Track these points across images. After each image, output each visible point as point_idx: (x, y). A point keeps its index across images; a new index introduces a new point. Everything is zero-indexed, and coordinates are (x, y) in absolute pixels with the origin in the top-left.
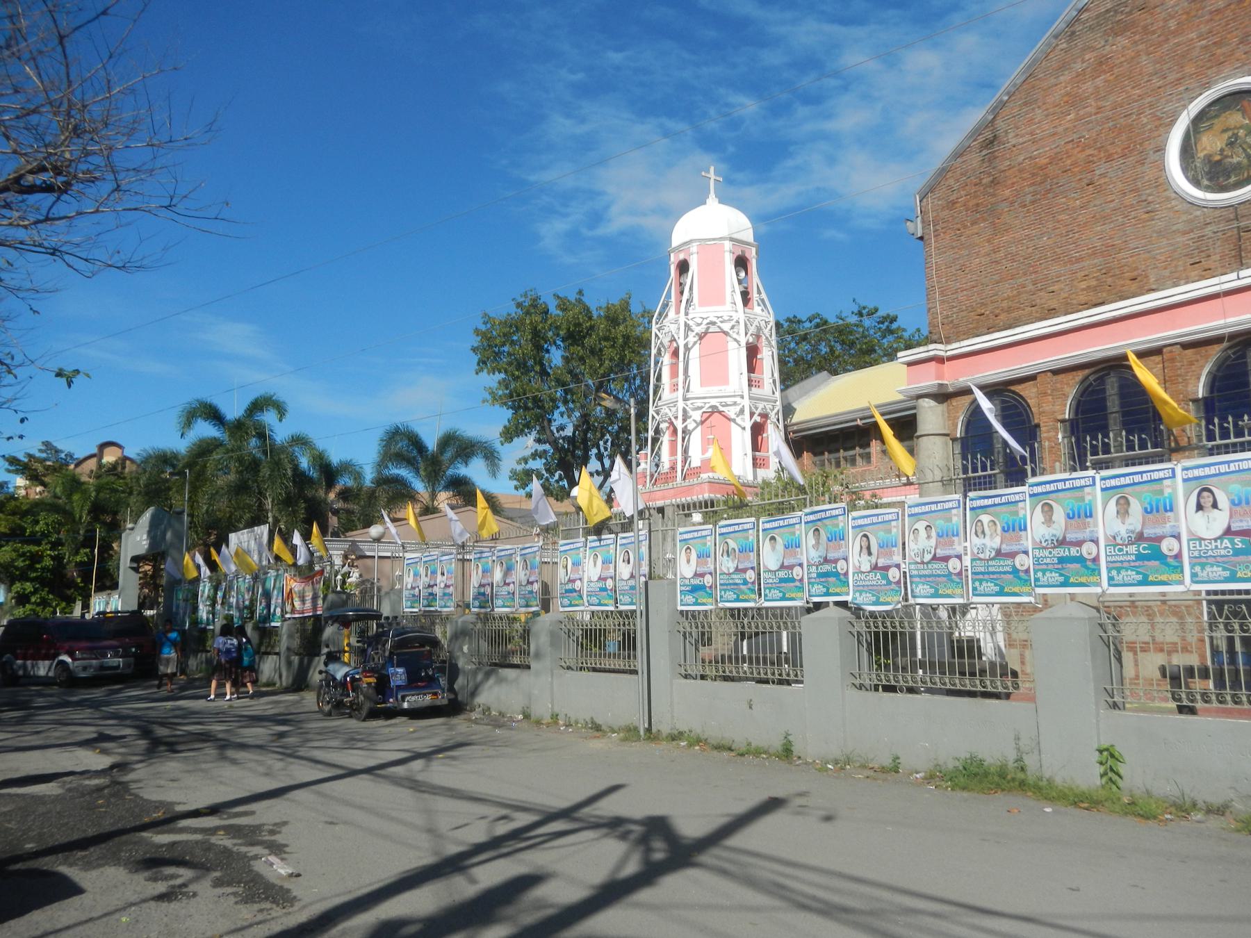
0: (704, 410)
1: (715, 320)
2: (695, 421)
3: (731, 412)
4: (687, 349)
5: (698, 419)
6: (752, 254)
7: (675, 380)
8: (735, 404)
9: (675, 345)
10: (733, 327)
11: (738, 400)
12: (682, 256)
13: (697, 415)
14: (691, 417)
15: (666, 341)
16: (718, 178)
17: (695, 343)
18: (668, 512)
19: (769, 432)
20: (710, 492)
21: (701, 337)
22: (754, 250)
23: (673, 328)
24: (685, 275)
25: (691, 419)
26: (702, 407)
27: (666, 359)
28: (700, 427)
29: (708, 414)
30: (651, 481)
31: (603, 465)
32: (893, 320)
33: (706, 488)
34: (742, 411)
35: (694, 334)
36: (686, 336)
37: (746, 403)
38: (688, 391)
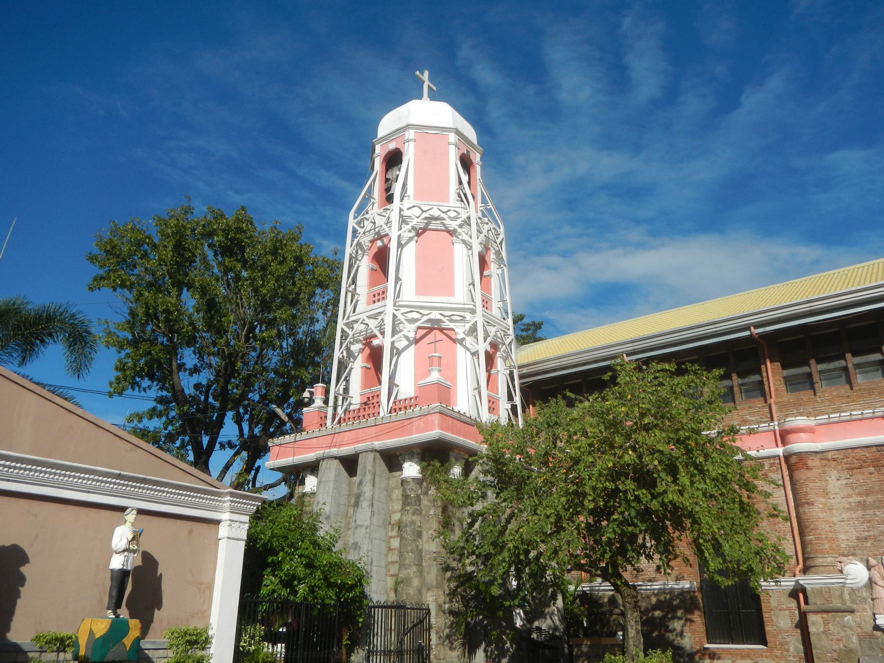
0: (418, 324)
1: (435, 213)
2: (407, 338)
3: (460, 331)
4: (400, 246)
5: (412, 335)
6: (476, 158)
7: (379, 288)
8: (463, 319)
9: (379, 243)
10: (460, 226)
11: (468, 315)
12: (392, 146)
13: (409, 330)
14: (401, 331)
15: (365, 240)
16: (432, 86)
17: (410, 239)
18: (366, 463)
19: (499, 368)
20: (442, 428)
21: (420, 232)
22: (478, 156)
23: (380, 221)
24: (395, 169)
25: (400, 335)
26: (417, 320)
27: (365, 265)
28: (413, 346)
29: (426, 331)
30: (333, 421)
31: (241, 429)
32: (538, 326)
33: (436, 422)
34: (473, 331)
35: (409, 227)
36: (400, 229)
37: (479, 318)
38: (398, 296)
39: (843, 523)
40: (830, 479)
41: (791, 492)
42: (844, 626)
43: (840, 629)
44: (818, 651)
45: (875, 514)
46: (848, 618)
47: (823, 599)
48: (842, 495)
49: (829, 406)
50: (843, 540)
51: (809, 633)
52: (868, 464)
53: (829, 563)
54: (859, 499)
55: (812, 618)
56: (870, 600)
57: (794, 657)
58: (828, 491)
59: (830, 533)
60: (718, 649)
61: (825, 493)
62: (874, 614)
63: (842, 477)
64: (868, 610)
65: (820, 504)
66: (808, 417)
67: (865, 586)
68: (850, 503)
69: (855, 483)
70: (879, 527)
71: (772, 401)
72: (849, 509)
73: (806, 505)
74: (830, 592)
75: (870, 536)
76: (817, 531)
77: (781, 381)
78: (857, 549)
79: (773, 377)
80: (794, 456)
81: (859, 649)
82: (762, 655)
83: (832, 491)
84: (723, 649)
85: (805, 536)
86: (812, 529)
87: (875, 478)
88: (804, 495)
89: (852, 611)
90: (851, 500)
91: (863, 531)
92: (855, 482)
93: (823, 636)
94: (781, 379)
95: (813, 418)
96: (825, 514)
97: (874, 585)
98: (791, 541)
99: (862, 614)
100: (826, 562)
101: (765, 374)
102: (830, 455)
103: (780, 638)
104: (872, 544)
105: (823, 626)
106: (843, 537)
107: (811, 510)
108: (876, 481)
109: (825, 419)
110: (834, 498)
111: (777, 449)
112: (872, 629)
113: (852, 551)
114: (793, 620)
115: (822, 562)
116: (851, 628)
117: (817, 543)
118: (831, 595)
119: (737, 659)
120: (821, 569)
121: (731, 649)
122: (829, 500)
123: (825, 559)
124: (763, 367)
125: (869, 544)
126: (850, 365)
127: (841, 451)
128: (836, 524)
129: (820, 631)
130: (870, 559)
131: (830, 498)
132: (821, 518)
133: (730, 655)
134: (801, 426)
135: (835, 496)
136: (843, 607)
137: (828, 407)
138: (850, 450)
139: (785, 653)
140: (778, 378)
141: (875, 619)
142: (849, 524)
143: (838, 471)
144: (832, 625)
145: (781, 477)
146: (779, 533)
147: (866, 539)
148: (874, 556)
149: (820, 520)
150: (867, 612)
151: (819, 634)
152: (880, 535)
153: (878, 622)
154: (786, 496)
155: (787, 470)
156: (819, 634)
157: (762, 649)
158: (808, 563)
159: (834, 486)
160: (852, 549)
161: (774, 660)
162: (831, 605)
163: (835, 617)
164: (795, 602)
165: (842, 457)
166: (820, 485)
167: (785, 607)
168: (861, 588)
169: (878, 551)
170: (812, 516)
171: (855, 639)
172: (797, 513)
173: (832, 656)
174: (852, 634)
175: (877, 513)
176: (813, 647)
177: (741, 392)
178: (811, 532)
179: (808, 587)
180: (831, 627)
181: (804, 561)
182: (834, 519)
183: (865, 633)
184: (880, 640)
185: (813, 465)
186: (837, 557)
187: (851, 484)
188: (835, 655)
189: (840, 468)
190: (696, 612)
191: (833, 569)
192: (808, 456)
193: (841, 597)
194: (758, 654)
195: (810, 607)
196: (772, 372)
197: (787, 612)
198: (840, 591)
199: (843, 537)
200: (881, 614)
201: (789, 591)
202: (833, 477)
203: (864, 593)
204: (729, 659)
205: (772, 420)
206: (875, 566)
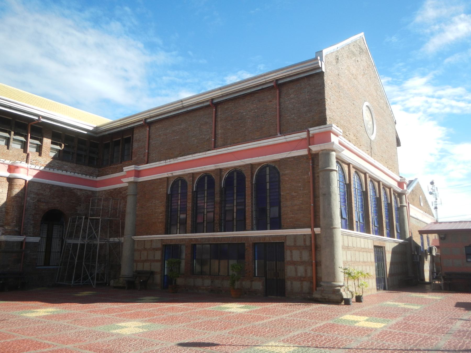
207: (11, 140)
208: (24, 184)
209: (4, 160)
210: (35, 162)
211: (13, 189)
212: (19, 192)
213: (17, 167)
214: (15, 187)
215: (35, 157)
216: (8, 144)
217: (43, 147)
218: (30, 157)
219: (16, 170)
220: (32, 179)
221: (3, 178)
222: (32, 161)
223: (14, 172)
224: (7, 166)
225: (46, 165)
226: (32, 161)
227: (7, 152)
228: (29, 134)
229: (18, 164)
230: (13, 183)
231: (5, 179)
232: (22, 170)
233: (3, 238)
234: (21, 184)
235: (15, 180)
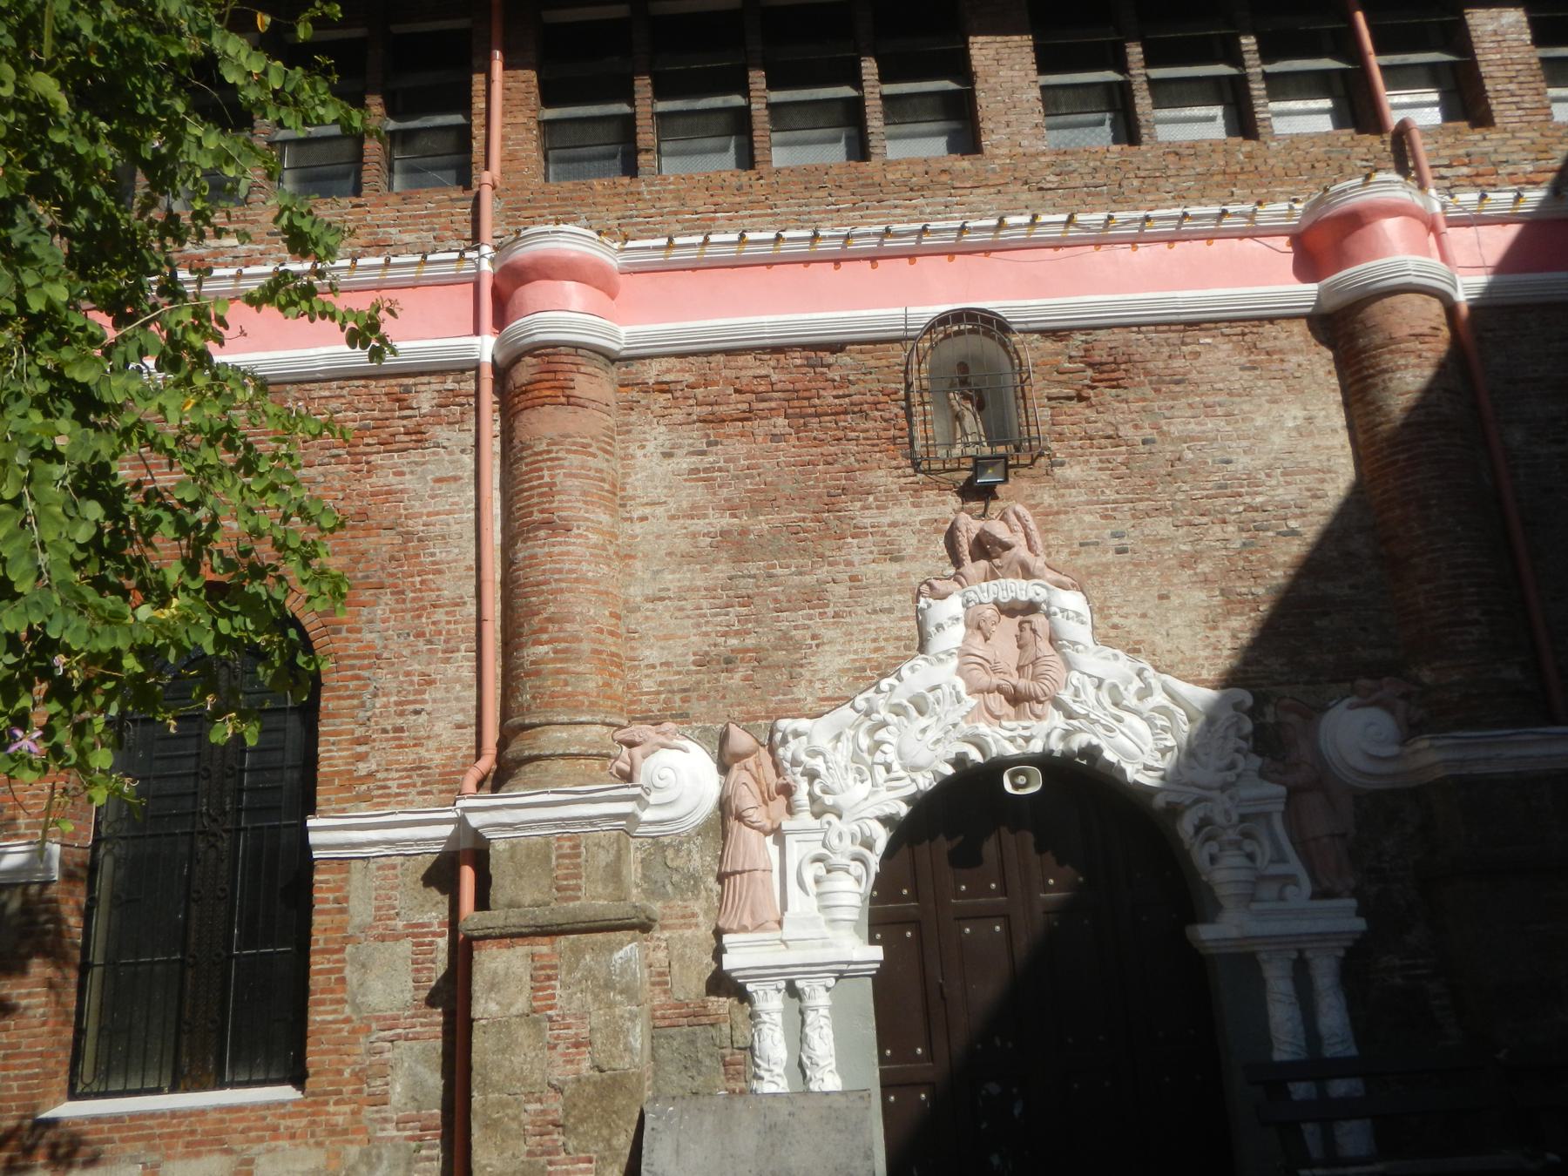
39: (660, 606)
40: (639, 453)
41: (497, 495)
42: (609, 985)
43: (589, 998)
44: (493, 1096)
45: (770, 576)
46: (628, 951)
47: (545, 882)
48: (672, 505)
49: (676, 213)
50: (653, 667)
51: (469, 1022)
52: (773, 404)
53: (592, 744)
54: (726, 521)
55: (491, 962)
56: (711, 881)
57: (401, 1123)
58: (630, 492)
59: (610, 640)
60: (96, 1120)
61: (616, 497)
62: (718, 933)
63: (680, 447)
64: (701, 918)
65: (596, 531)
66: (599, 233)
67: (703, 830)
68: (694, 535)
69: (720, 470)
70: (777, 620)
71: (486, 177)
72: (688, 558)
73: (542, 533)
74: (578, 856)
75: (747, 650)
76: (568, 626)
77: (529, 130)
78: (694, 695)
79: (504, 114)
80: (528, 360)
81: (647, 1067)
82: (275, 1129)
83: (639, 492)
84: (116, 1119)
85: (520, 647)
86: (549, 620)
87: (788, 450)
88: (542, 495)
89: (645, 927)
90: (699, 525)
91: (725, 634)
92: (722, 464)
93: (522, 1033)
94: (533, 124)
95: (616, 246)
96: (605, 569)
97: (733, 824)
98: (468, 674)
99: (676, 934)
100: (580, 742)
101: (479, 104)
102: (651, 372)
103: (361, 1049)
104: (746, 679)
105: (527, 992)
106: (652, 655)
107: (556, 549)
108: (788, 465)
109: (656, 248)
110: (643, 519)
111: (476, 340)
112: (702, 987)
113: (678, 703)
114: (424, 975)
115: (568, 742)
116: (629, 992)
117: (558, 672)
118: (577, 866)
119: (168, 1157)
120: (559, 766)
121: (152, 1115)
122: (627, 525)
123: (579, 730)
124: (478, 80)
125: (736, 679)
126: (758, 108)
127: (691, 359)
128: (635, 609)
129: (514, 1010)
130: (733, 727)
131: (631, 519)
132: (588, 581)
133: (140, 1144)
134: (573, 255)
135: (648, 510)
136: (616, 911)
137: (672, 218)
138: (721, 358)
139: (368, 1112)
140: (522, 120)
141: (719, 952)
142: (681, 609)
143: (672, 426)
144: (565, 986)
145: (472, 441)
146: (430, 642)
147: (728, 661)
148: (748, 722)
149: (582, 587)
150: (697, 925)
151: (508, 1025)
152: (775, 648)
153: (729, 962)
154: (478, 509)
155: (497, 416)
156: (508, 1025)
157: (282, 1104)
158: (513, 750)
159: (651, 478)
160: (677, 697)
161: (319, 1144)
162: (571, 904)
163: (577, 952)
164: (445, 900)
165: (692, 379)
166: (604, 465)
167: (400, 924)
168: (689, 838)
169: (763, 700)
170: (560, 571)
171: (638, 1037)
172: (508, 563)
173: (543, 1112)
174: (633, 1017)
175: (778, 571)
176: (476, 1079)
177: (391, 170)
178: (543, 630)
179: (499, 844)
180: (558, 992)
181: (502, 745)
182: (632, 590)
183: (680, 1005)
184: (726, 1029)
185: (592, 396)
186: (621, 727)
187: (706, 470)
188: (556, 1105)
189: (678, 415)
190: (39, 969)
191: (603, 768)
192: (578, 360)
193: (614, 873)
194: (264, 1124)
195: (494, 918)
196: (506, 99)
197: (406, 946)
198: (613, 852)
199: (652, 655)
200: (744, 929)
201: (430, 860)
202: (650, 447)
203: (696, 856)
204: (134, 1160)
205: (476, 238)
206: (747, 755)
207: (1258, 88)
208: (1445, 332)
209: (1248, 208)
210: (1465, 170)
211: (1378, 380)
212: (1428, 390)
213: (1355, 221)
214: (1387, 360)
215: (1450, 140)
216: (1244, 123)
217: (1483, 69)
218: (1422, 147)
219: (1353, 244)
220: (1490, 288)
221: (1284, 323)
222: (1443, 171)
223: (1342, 261)
224: (1282, 243)
225: (1551, 176)
226: (1443, 171)
227: (1249, 156)
228: (1360, 17)
229: (1354, 194)
230: (1362, 342)
231: (1300, 329)
232: (1391, 227)
233: (1433, 757)
234: (1426, 330)
235: (1376, 308)
